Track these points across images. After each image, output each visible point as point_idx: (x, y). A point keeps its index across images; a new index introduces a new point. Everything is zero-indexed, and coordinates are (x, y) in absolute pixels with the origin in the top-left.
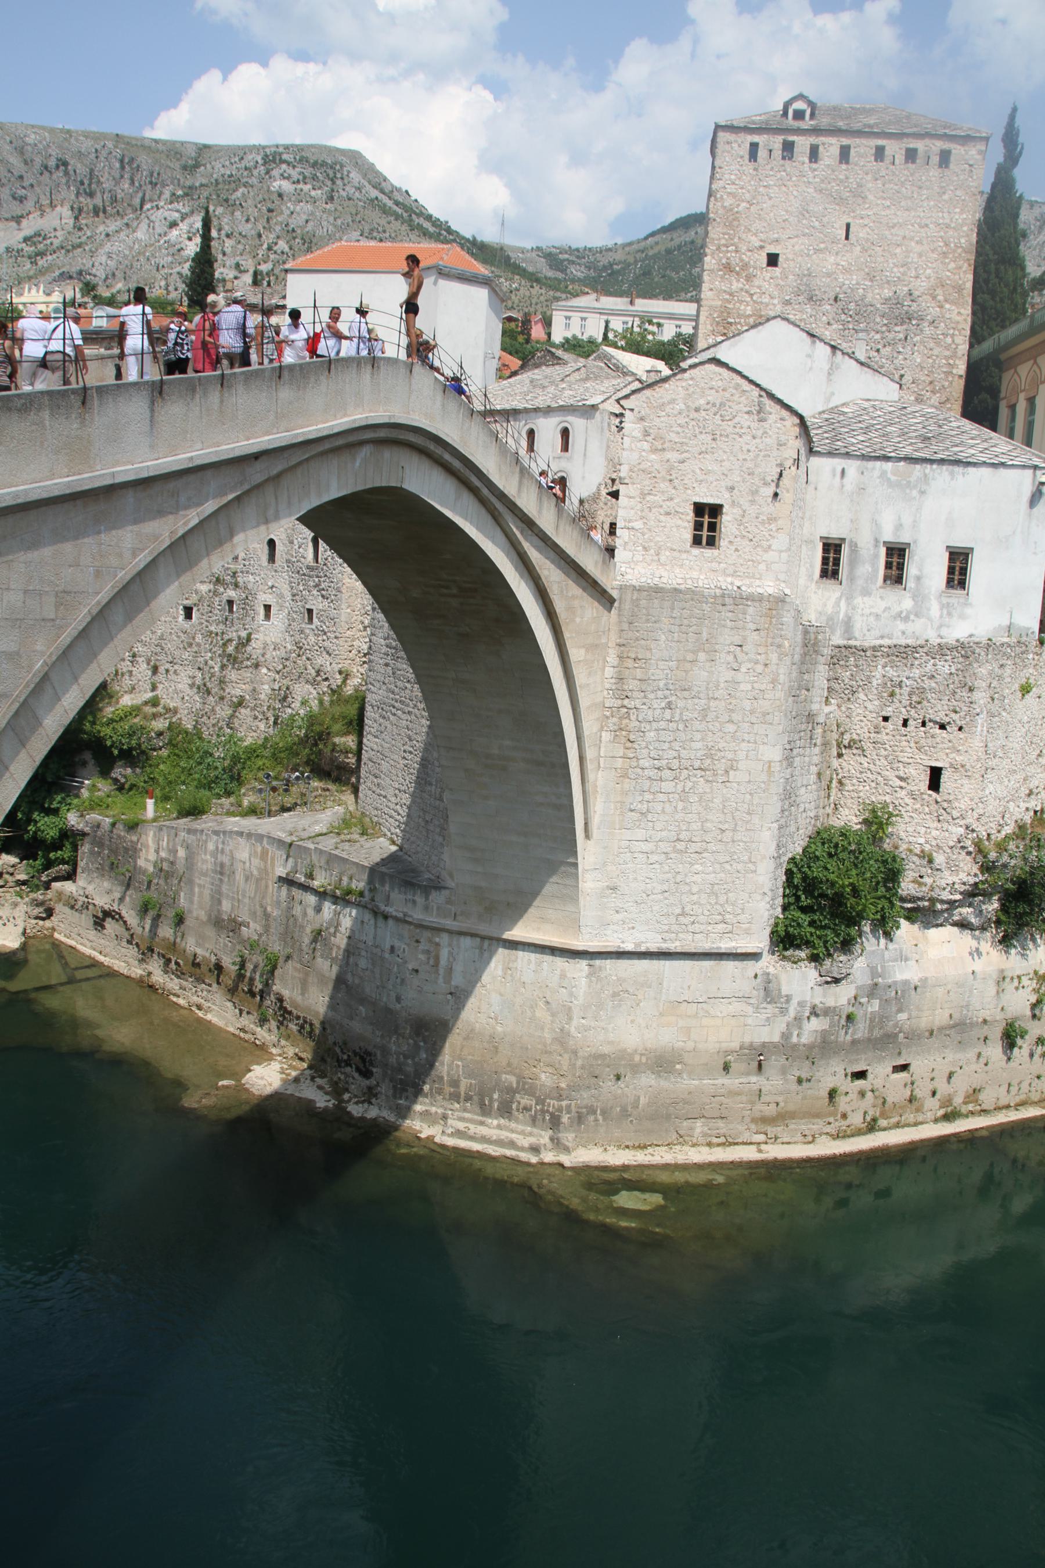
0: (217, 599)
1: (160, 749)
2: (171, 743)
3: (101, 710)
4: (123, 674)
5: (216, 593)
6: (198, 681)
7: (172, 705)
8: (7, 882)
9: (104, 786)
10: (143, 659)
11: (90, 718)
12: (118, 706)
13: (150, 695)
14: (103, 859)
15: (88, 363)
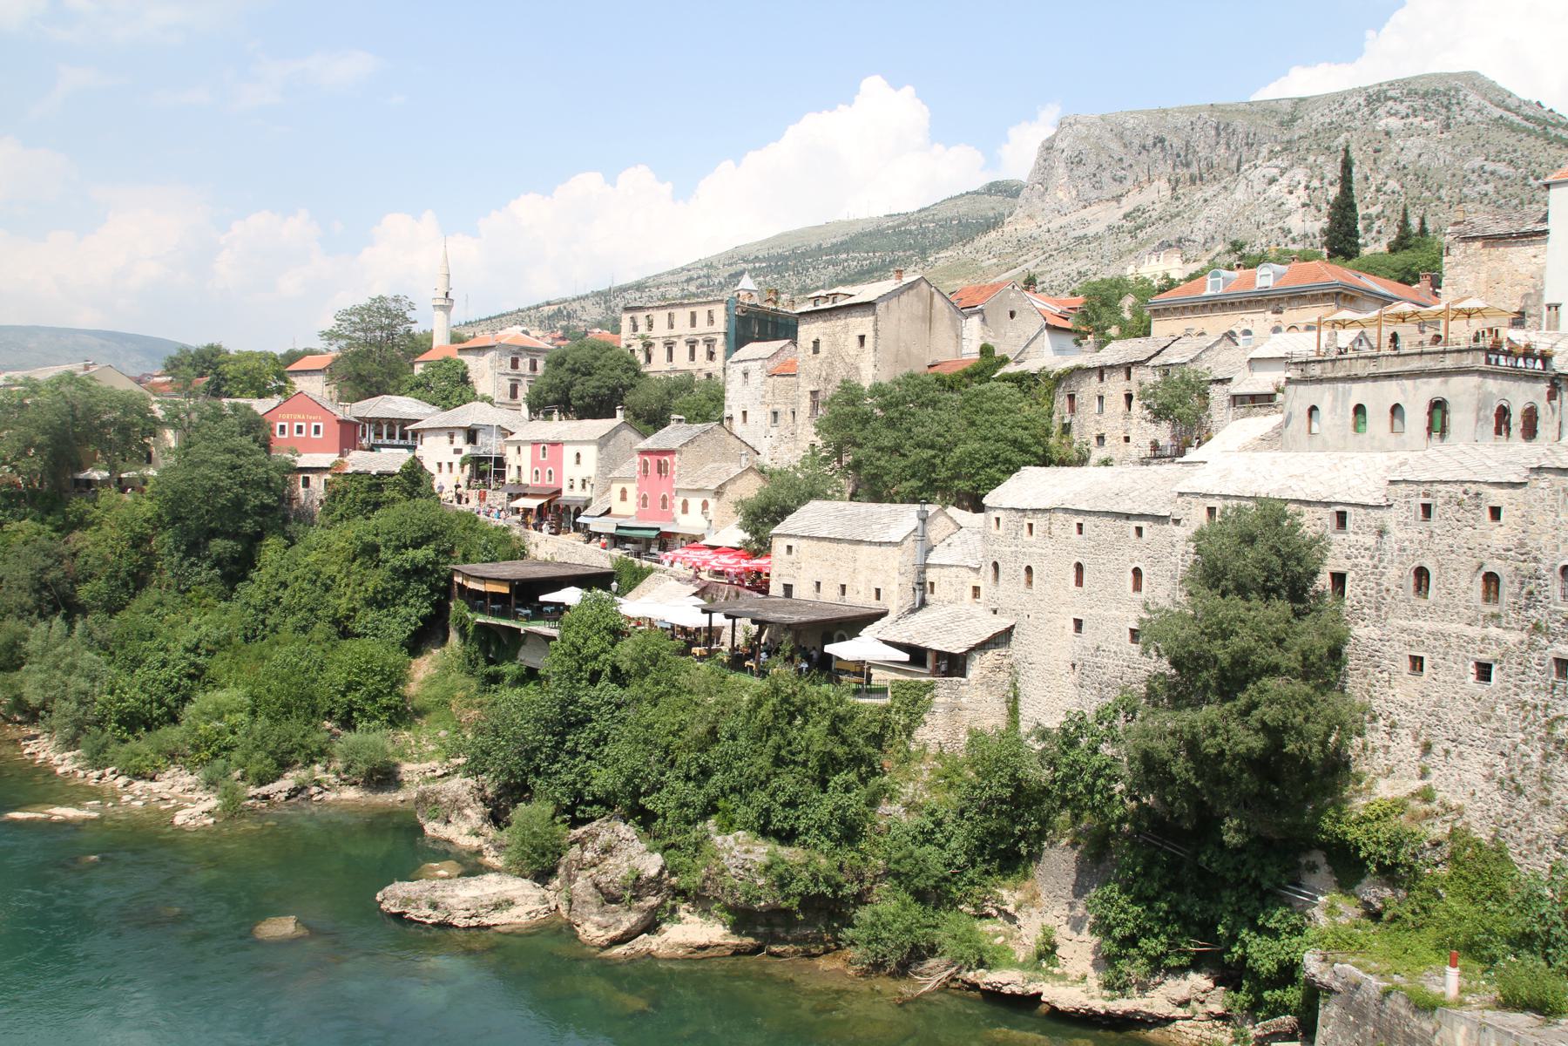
0: (1536, 655)
1: (1436, 865)
2: (1453, 857)
3: (1346, 801)
4: (1374, 750)
5: (1532, 646)
6: (1501, 770)
7: (1454, 803)
8: (1195, 1013)
9: (1348, 910)
10: (1407, 731)
11: (1331, 812)
12: (1373, 799)
13: (1418, 784)
14: (1363, 1036)
15: (1315, 333)
